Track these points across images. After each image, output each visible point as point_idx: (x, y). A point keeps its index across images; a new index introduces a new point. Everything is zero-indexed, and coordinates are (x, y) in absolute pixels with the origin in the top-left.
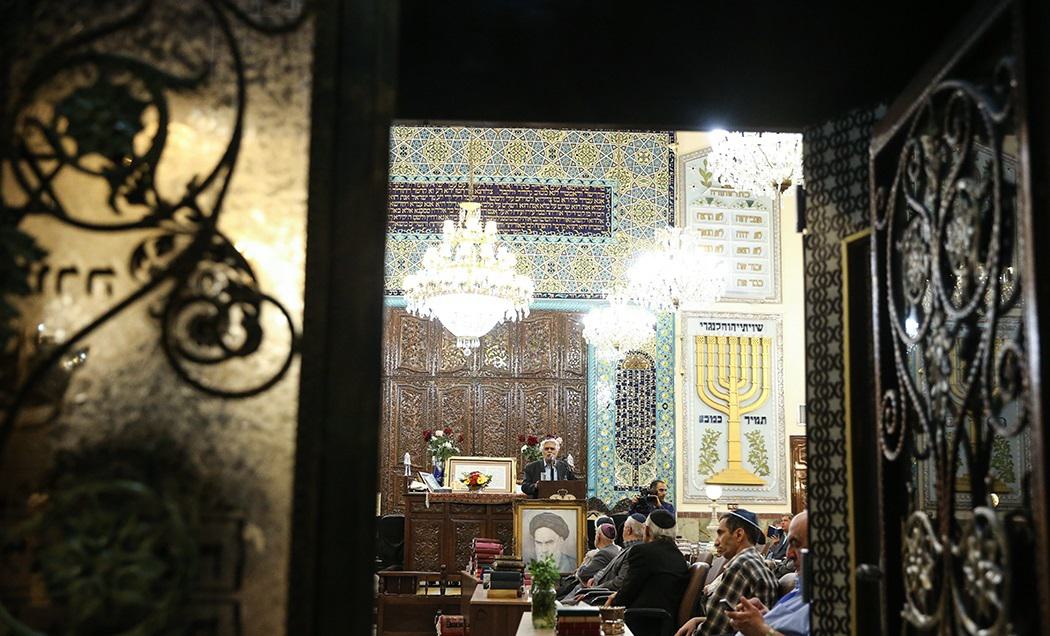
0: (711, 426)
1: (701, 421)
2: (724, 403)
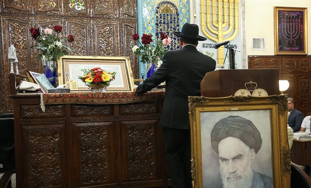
2: (216, 36)
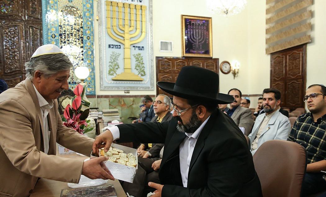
0: (115, 50)
1: (110, 46)
